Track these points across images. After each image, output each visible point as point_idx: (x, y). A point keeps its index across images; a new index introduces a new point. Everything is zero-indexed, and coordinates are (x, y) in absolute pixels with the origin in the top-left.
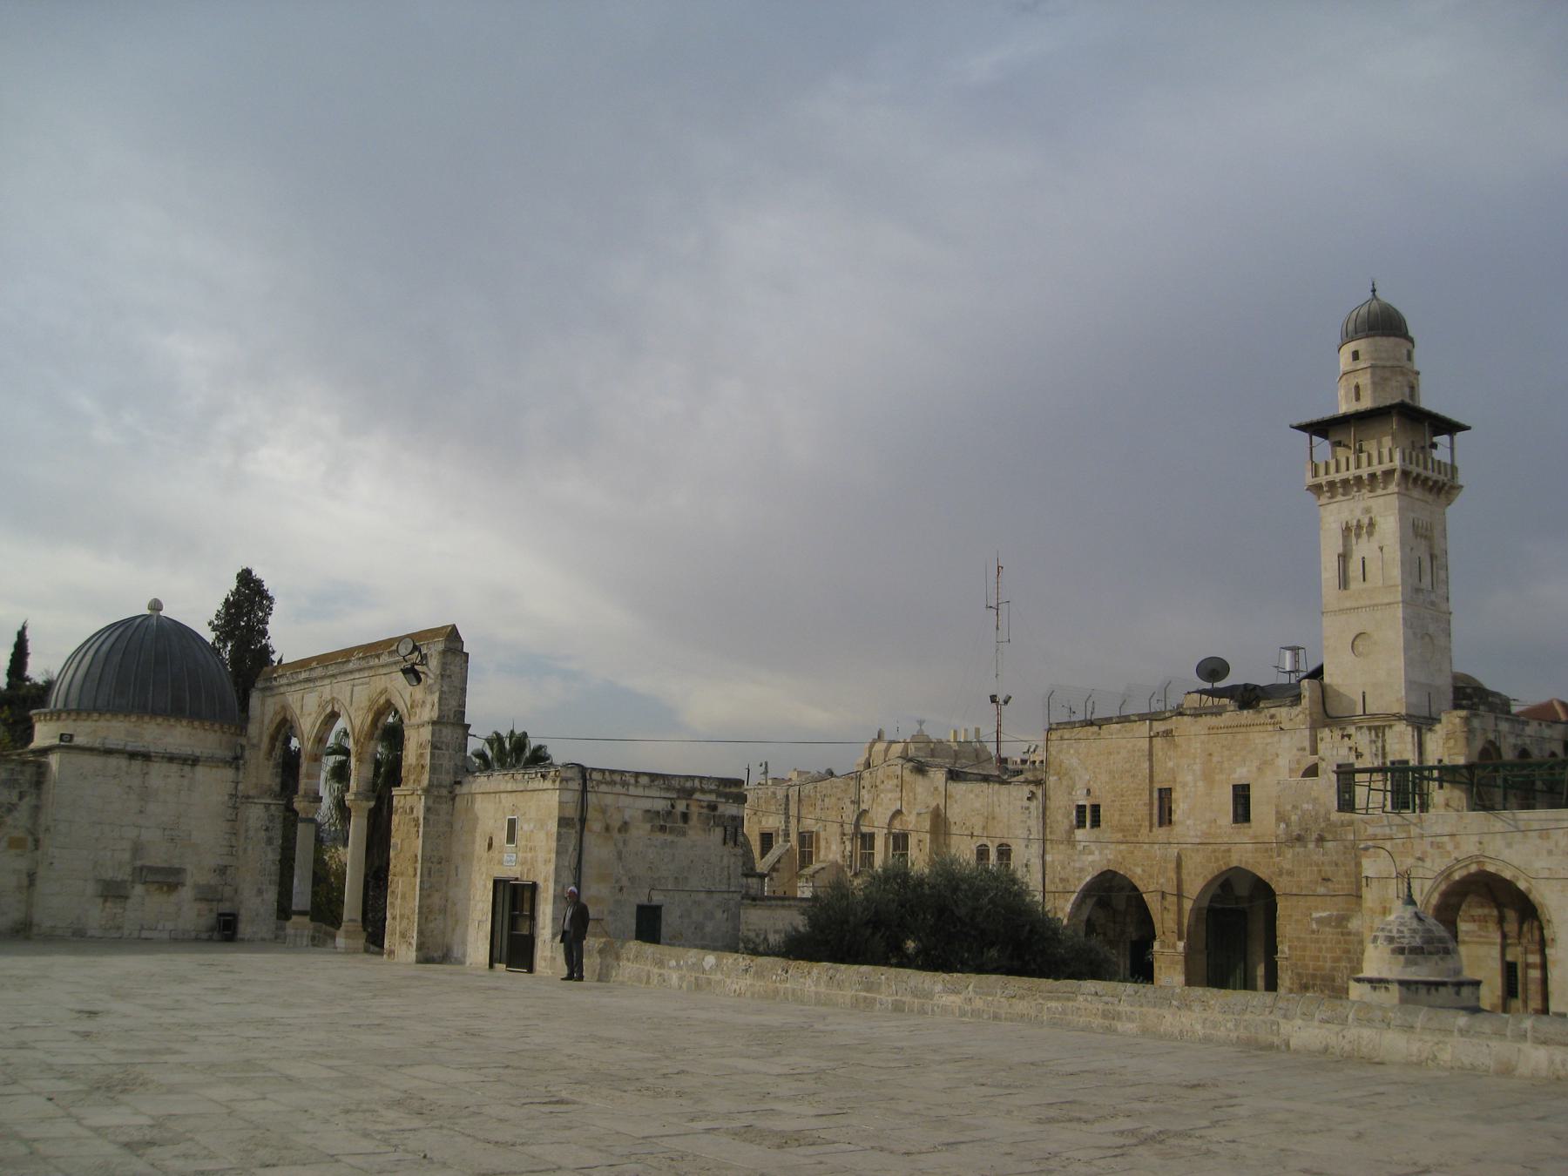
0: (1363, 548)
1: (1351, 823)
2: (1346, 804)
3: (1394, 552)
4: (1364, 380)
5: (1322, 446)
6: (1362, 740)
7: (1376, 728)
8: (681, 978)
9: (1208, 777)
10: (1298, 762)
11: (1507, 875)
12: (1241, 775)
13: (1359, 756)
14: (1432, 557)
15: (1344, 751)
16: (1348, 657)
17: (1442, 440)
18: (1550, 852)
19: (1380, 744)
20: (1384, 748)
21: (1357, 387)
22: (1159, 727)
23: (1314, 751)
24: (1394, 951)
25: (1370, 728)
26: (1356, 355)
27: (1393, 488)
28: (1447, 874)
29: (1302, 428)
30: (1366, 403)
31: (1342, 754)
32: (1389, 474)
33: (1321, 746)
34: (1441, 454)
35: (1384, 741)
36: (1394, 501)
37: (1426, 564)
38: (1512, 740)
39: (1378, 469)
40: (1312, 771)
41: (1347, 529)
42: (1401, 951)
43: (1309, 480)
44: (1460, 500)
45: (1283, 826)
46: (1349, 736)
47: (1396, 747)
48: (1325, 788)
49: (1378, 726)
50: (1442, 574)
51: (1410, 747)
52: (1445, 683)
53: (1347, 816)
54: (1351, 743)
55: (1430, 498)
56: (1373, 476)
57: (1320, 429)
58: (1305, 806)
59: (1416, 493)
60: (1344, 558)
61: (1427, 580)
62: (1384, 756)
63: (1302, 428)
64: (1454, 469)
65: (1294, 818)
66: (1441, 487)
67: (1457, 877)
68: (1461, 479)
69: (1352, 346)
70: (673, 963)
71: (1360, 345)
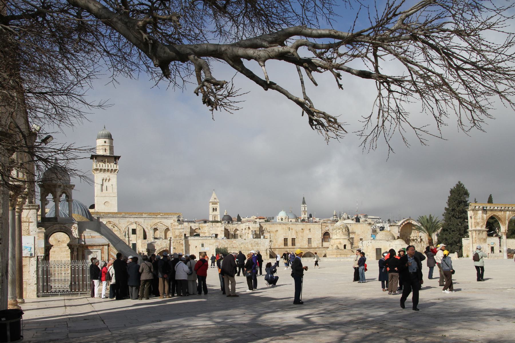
3: (115, 186)
4: (108, 148)
21: (105, 149)
26: (105, 142)
27: (116, 173)
30: (108, 153)
32: (115, 170)
36: (116, 176)
41: (103, 180)
43: (95, 167)
56: (112, 170)
69: (105, 140)
71: (107, 140)
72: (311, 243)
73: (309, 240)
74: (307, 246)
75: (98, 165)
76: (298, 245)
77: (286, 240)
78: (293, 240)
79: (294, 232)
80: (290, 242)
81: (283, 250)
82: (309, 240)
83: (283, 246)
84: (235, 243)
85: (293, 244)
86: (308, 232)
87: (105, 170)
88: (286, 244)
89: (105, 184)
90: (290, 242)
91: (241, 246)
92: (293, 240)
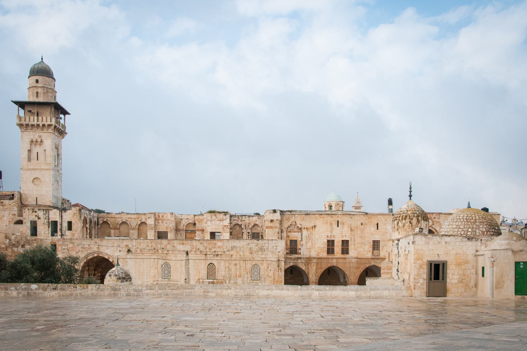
1: (35, 240)
5: (22, 112)
7: (46, 210)
8: (18, 293)
10: (13, 219)
11: (106, 257)
13: (39, 218)
15: (34, 217)
18: (120, 251)
19: (47, 215)
20: (48, 216)
23: (21, 215)
24: (117, 279)
25: (43, 210)
28: (86, 257)
29: (16, 103)
31: (33, 218)
33: (24, 214)
35: (48, 214)
40: (20, 222)
42: (120, 278)
45: (8, 240)
46: (36, 212)
47: (54, 216)
48: (26, 228)
49: (47, 209)
51: (58, 217)
53: (34, 238)
54: (36, 214)
57: (22, 105)
58: (17, 234)
62: (49, 219)
63: (16, 103)
65: (13, 238)
67: (90, 258)
70: (13, 288)
72: (378, 249)
74: (369, 255)
75: (27, 118)
76: (353, 253)
77: (331, 244)
78: (345, 243)
80: (338, 248)
81: (325, 261)
83: (324, 254)
84: (219, 247)
85: (345, 250)
86: (373, 228)
87: (33, 126)
88: (330, 250)
90: (338, 248)
91: (231, 253)
92: (345, 243)
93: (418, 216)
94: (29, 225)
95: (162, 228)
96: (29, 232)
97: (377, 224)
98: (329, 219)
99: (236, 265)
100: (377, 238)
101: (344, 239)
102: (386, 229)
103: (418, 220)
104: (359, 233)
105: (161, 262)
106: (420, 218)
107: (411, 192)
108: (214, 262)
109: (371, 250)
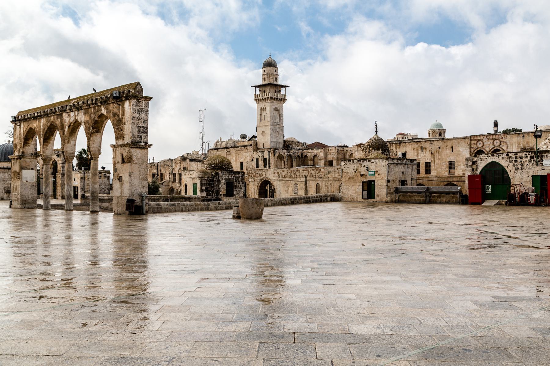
0: (264, 114)
2: (257, 166)
3: (269, 115)
6: (260, 154)
9: (236, 161)
12: (242, 160)
14: (279, 115)
16: (261, 136)
17: (284, 88)
22: (228, 150)
27: (269, 101)
30: (266, 82)
31: (257, 157)
32: (268, 98)
34: (283, 92)
37: (278, 116)
38: (286, 154)
39: (266, 97)
44: (287, 102)
48: (254, 163)
50: (282, 118)
52: (281, 141)
55: (279, 102)
59: (275, 102)
60: (261, 115)
61: (278, 120)
64: (285, 95)
66: (283, 99)
68: (287, 98)
73: (451, 165)
74: (446, 174)
76: (433, 173)
78: (428, 165)
79: (428, 153)
80: (422, 169)
82: (451, 165)
85: (428, 171)
86: (449, 151)
89: (264, 114)
92: (428, 165)
93: (370, 147)
94: (255, 161)
95: (330, 158)
96: (255, 166)
97: (452, 147)
98: (415, 146)
99: (331, 184)
100: (452, 159)
101: (426, 161)
102: (459, 151)
103: (369, 150)
104: (438, 155)
105: (294, 183)
106: (371, 149)
107: (376, 128)
108: (320, 183)
109: (448, 169)
